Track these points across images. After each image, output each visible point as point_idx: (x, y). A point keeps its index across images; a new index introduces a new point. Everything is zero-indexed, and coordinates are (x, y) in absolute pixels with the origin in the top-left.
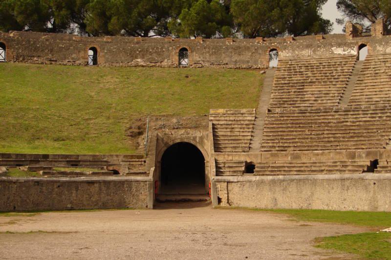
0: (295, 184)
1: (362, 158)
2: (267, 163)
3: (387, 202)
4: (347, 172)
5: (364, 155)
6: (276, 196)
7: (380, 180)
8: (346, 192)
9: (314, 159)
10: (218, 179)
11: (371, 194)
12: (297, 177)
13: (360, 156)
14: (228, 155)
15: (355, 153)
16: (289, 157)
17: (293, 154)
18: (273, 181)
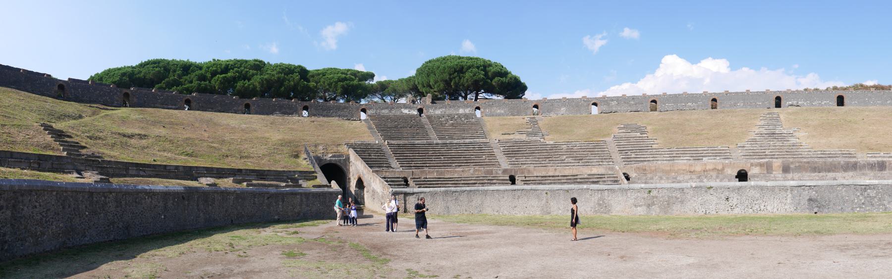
0: (465, 194)
1: (499, 174)
2: (419, 178)
3: (561, 208)
4: (497, 185)
5: (500, 172)
6: (448, 204)
7: (554, 190)
8: (516, 200)
9: (456, 176)
10: (397, 191)
11: (544, 202)
12: (468, 188)
13: (497, 173)
14: (386, 172)
15: (492, 171)
16: (435, 173)
17: (437, 171)
18: (446, 192)
